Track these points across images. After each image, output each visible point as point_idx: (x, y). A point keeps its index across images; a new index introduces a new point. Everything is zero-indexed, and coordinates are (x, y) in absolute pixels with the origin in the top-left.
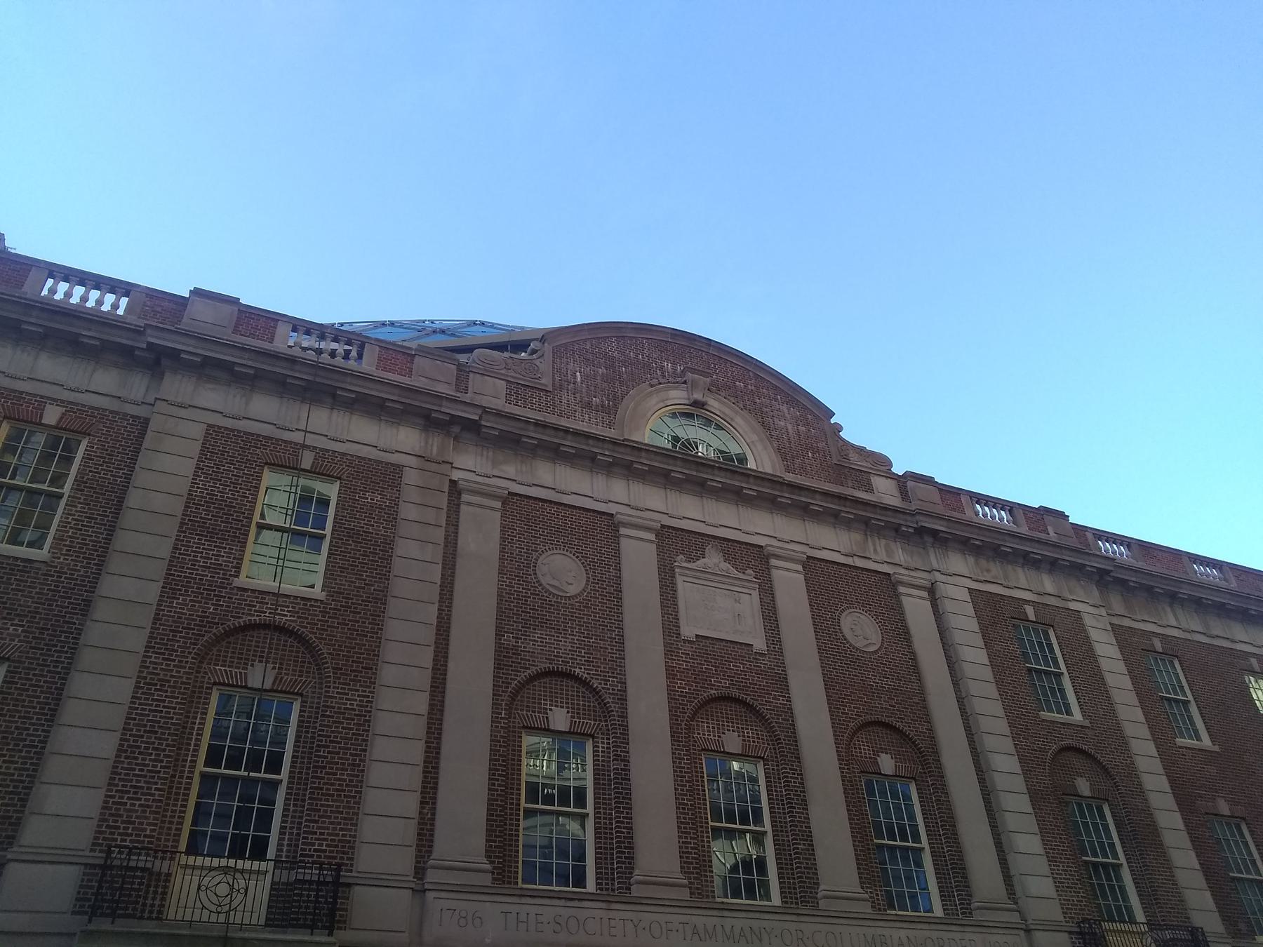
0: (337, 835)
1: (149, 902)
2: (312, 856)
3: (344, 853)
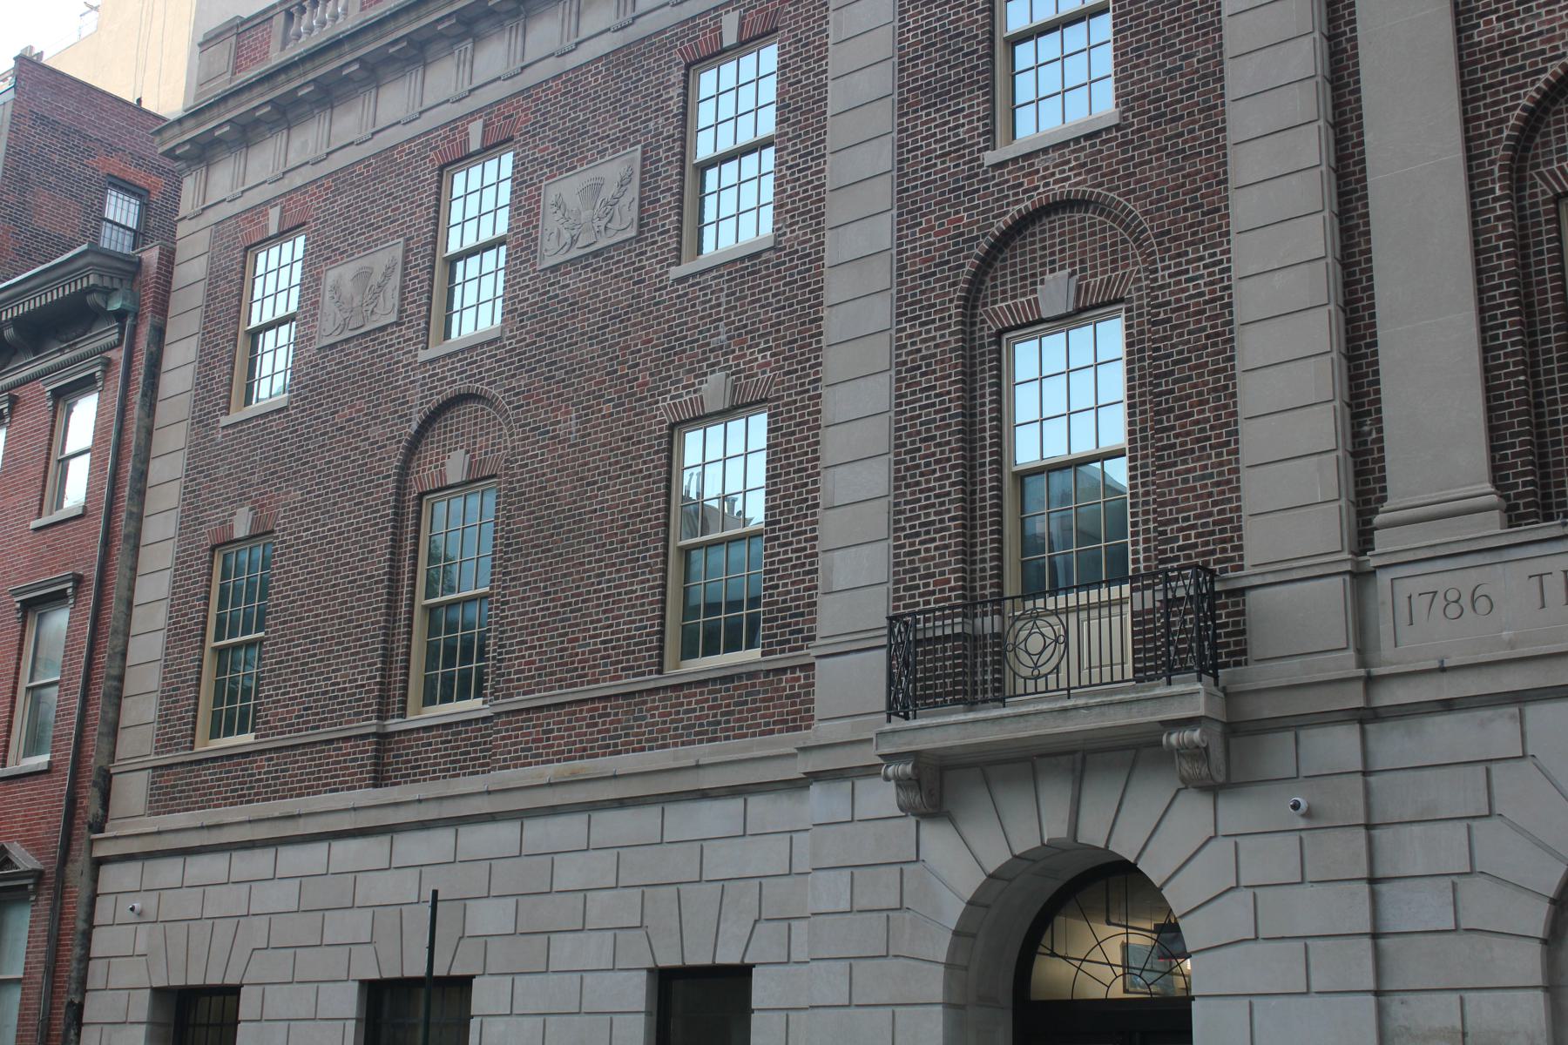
0: (1210, 514)
1: (979, 678)
2: (1177, 559)
3: (1224, 541)
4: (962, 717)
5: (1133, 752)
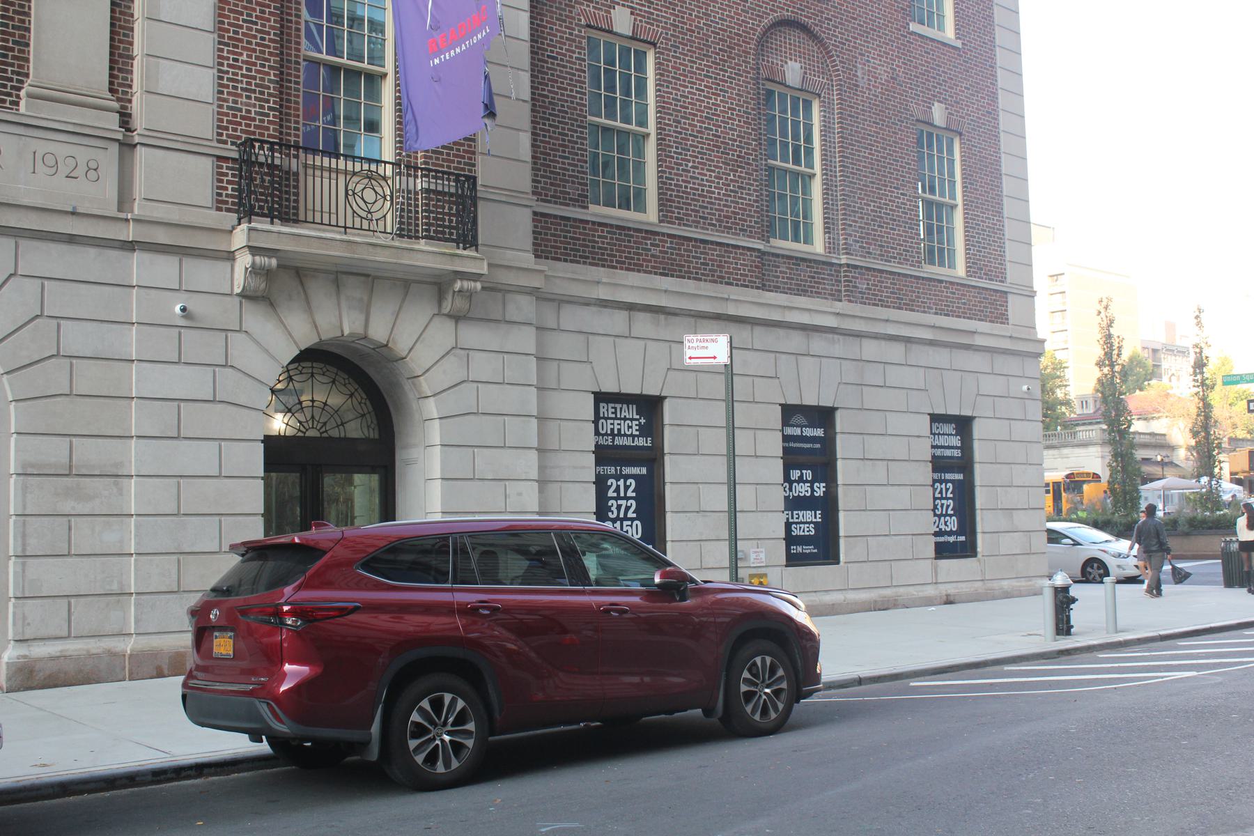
4: (268, 227)
5: (406, 284)
